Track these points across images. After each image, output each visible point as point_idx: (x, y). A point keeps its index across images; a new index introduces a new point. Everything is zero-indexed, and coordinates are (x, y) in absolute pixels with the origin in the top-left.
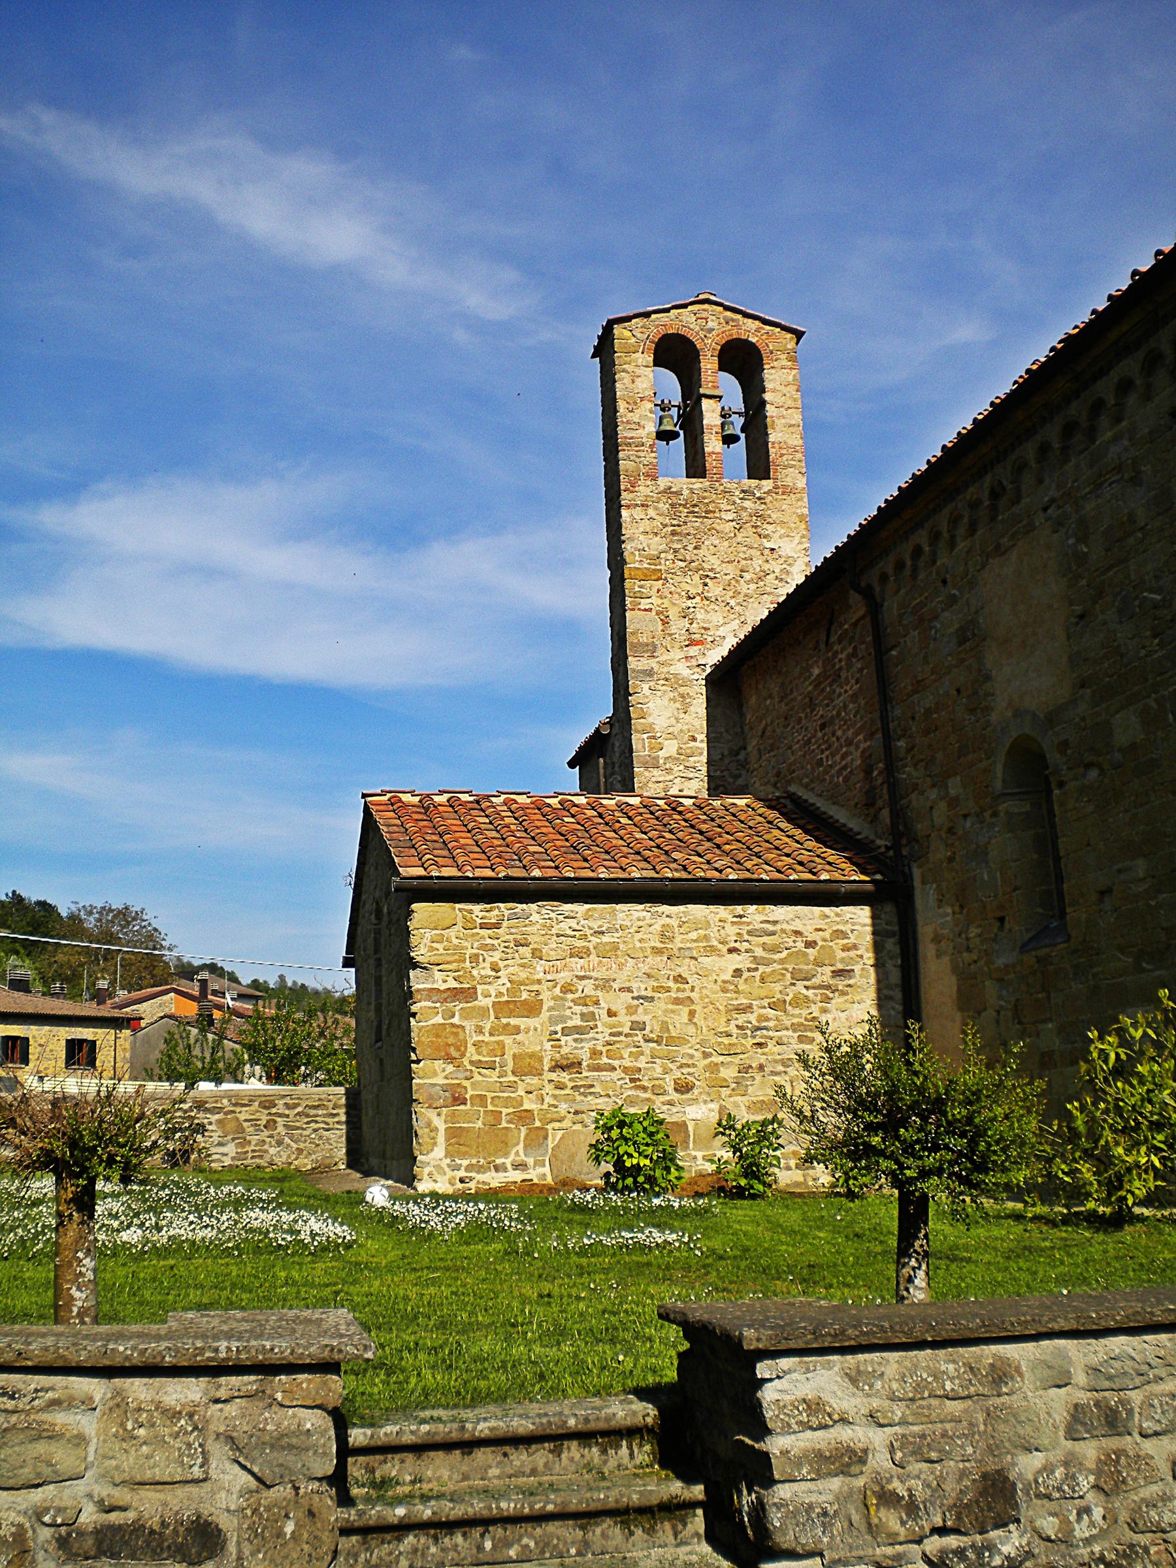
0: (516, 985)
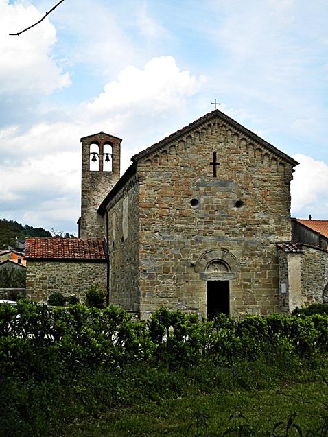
0: (43, 275)
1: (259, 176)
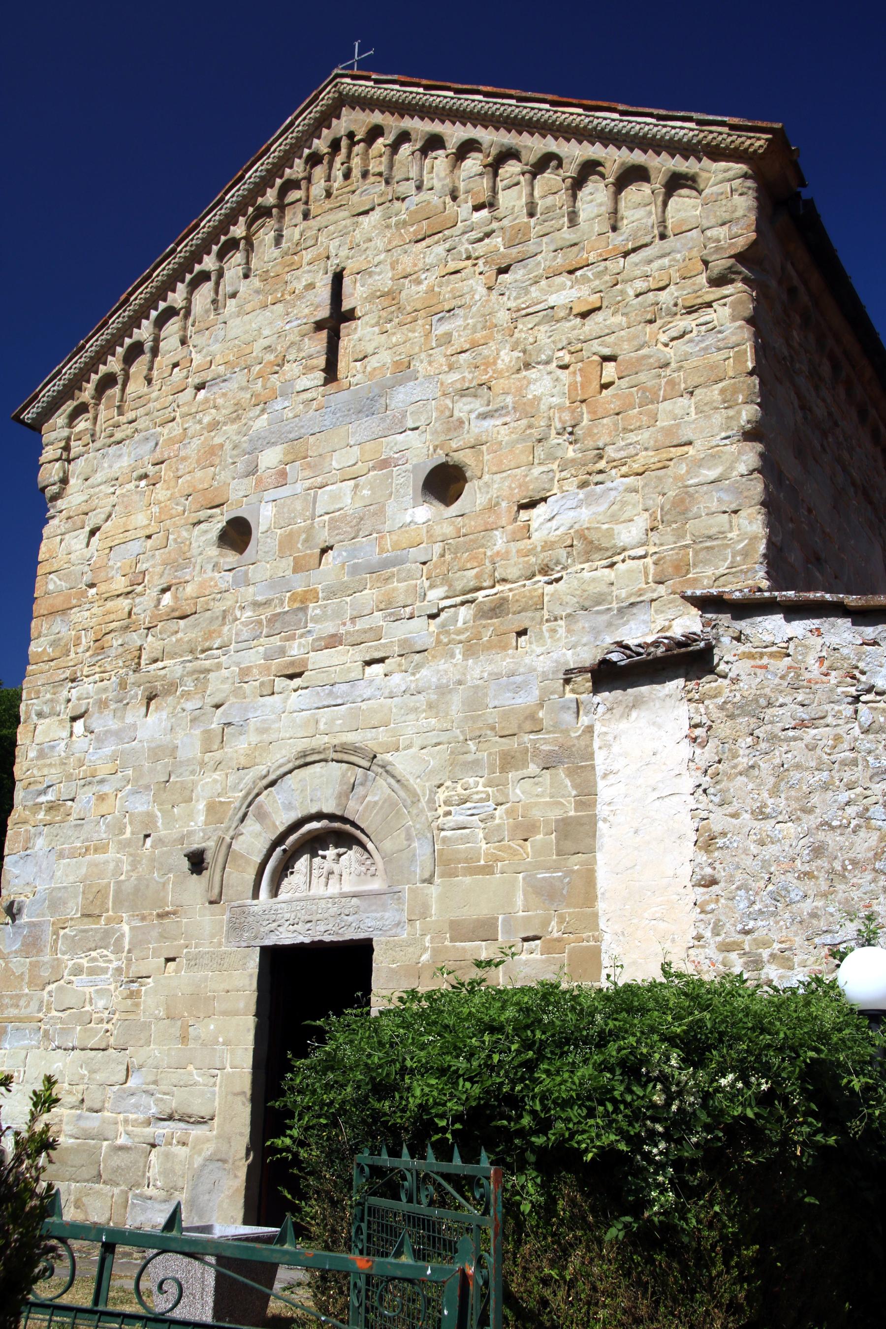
1: (552, 300)
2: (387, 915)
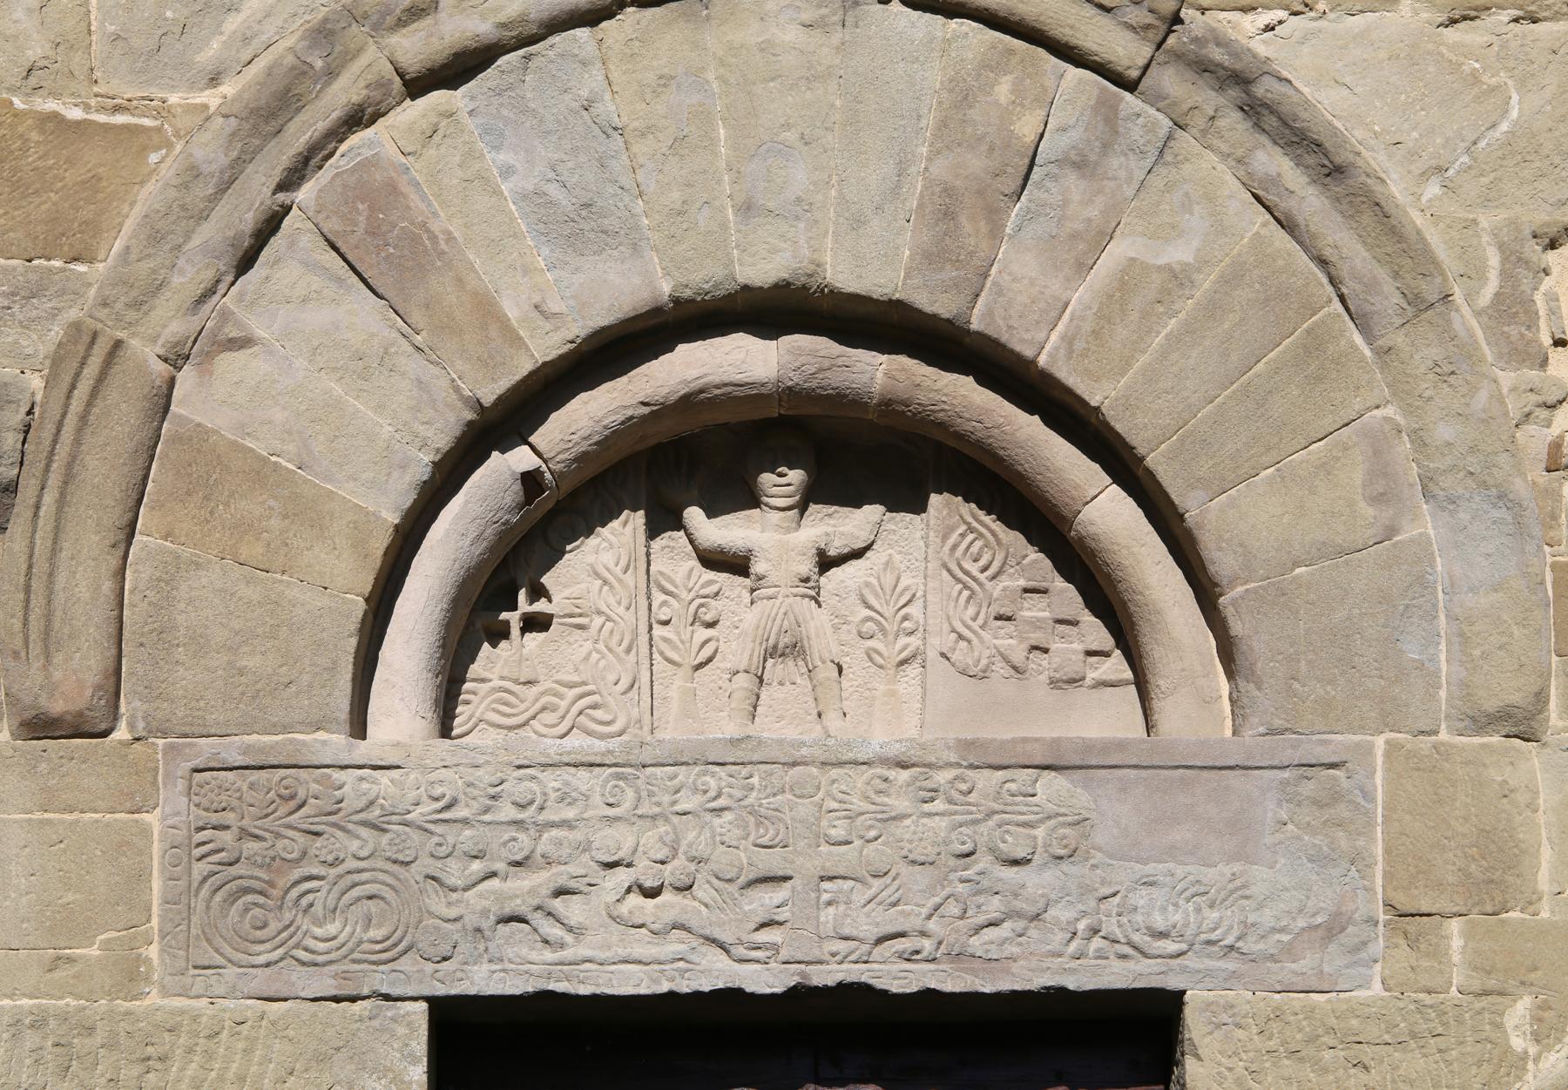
2: (1261, 877)
